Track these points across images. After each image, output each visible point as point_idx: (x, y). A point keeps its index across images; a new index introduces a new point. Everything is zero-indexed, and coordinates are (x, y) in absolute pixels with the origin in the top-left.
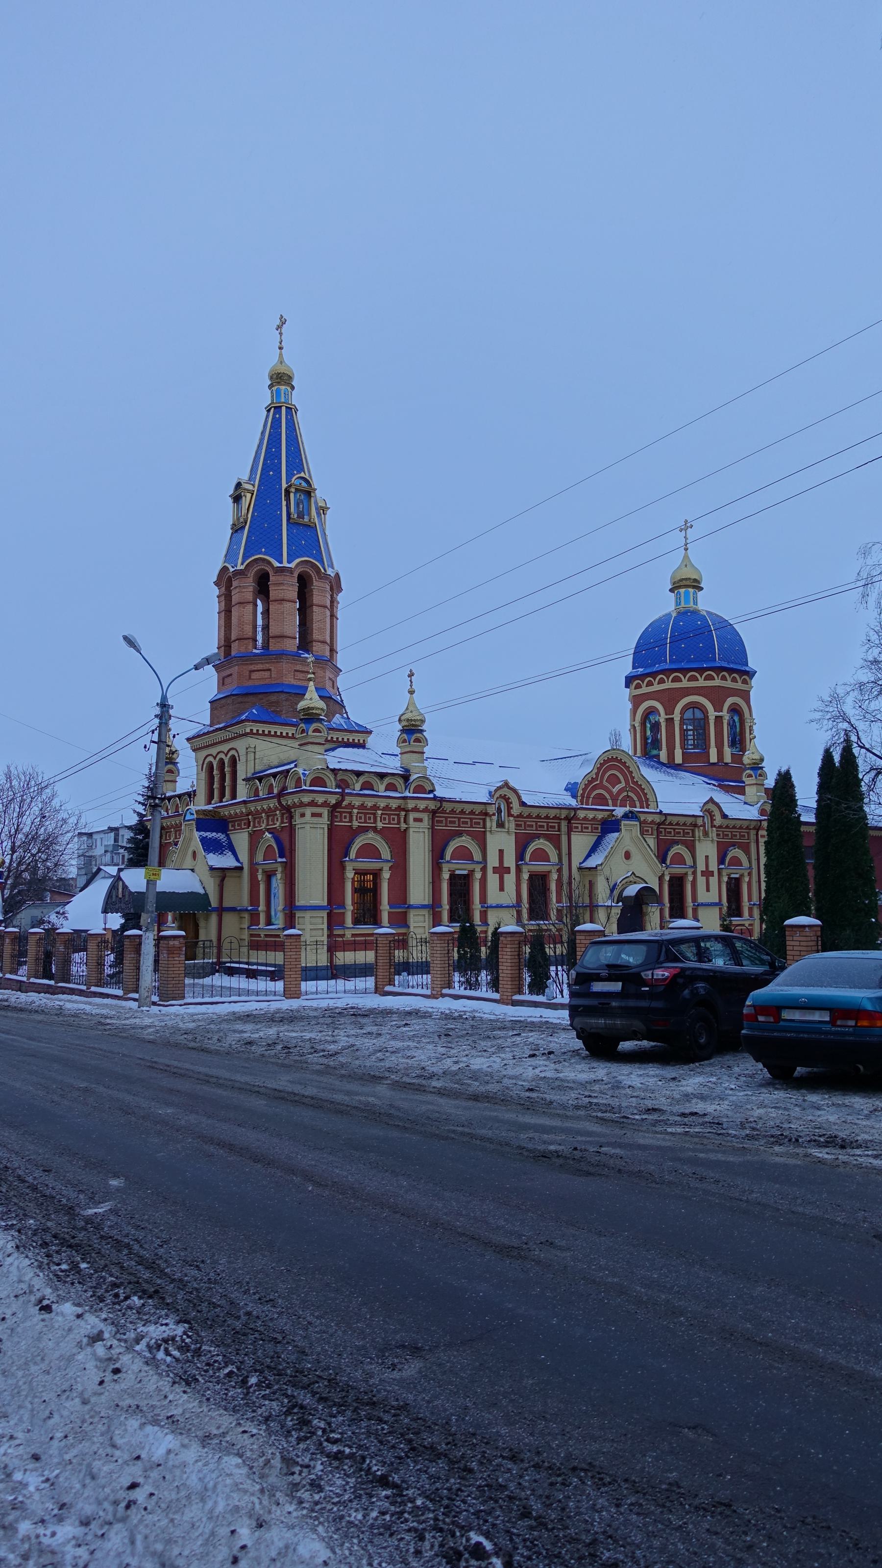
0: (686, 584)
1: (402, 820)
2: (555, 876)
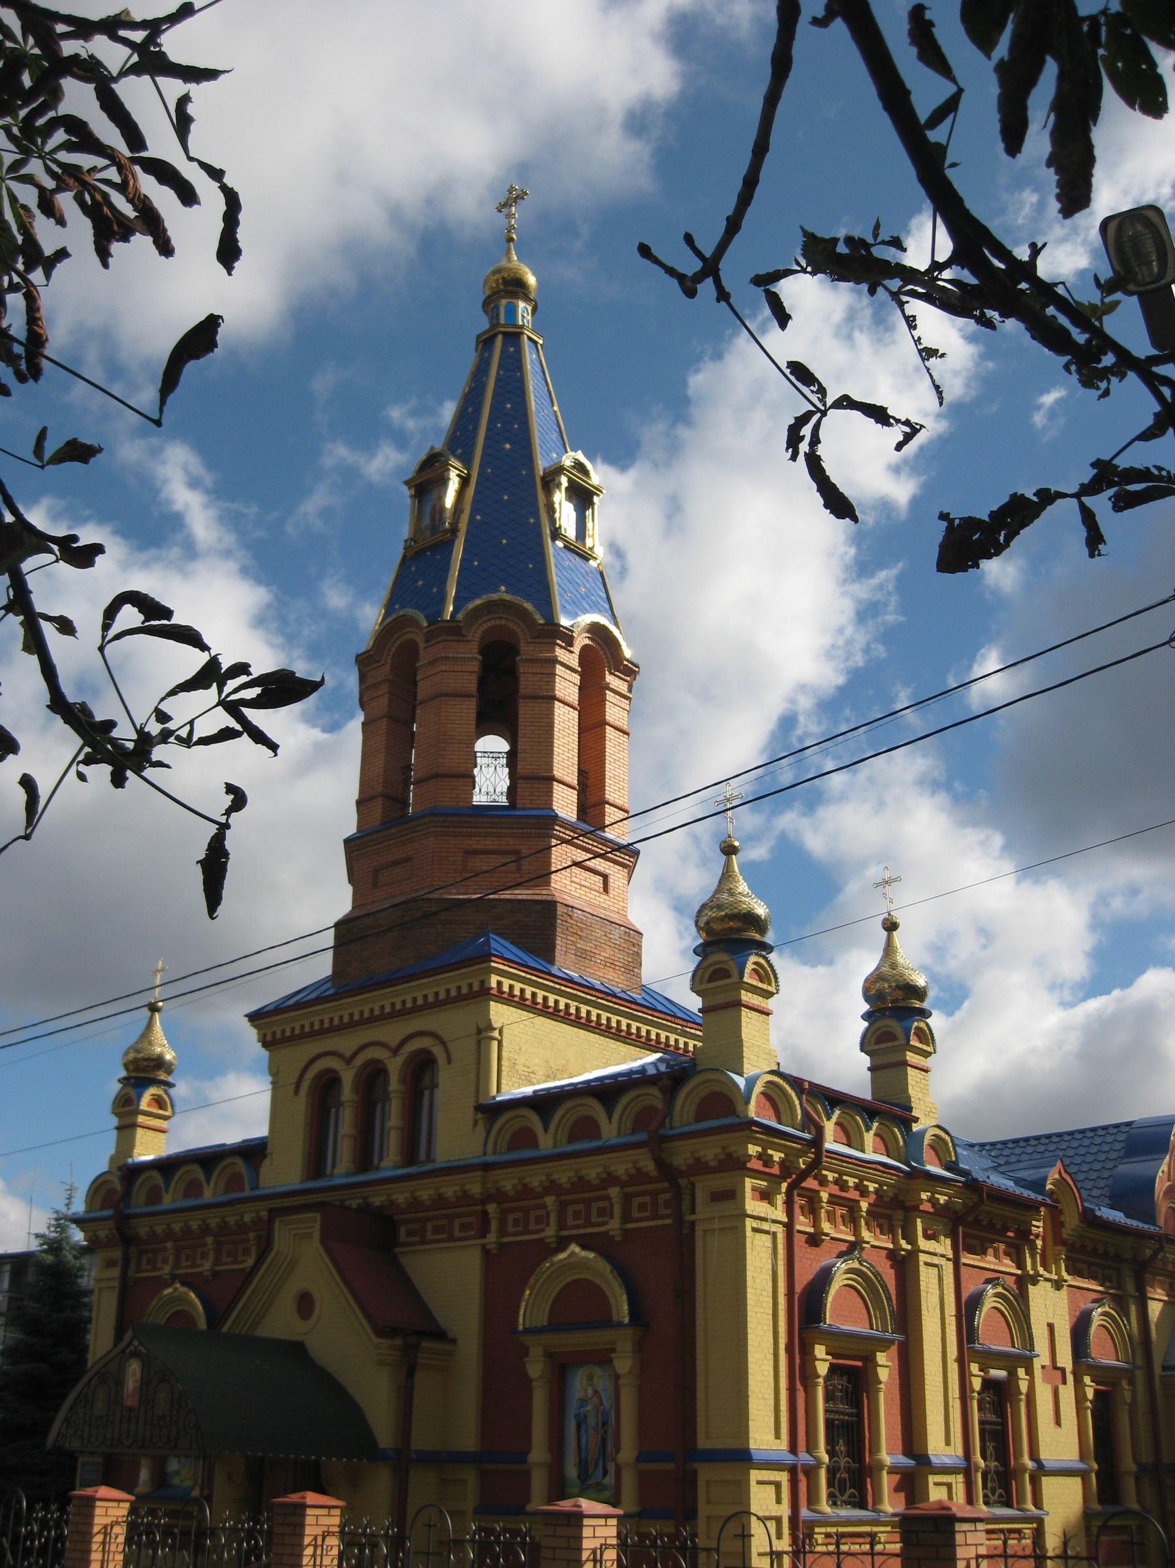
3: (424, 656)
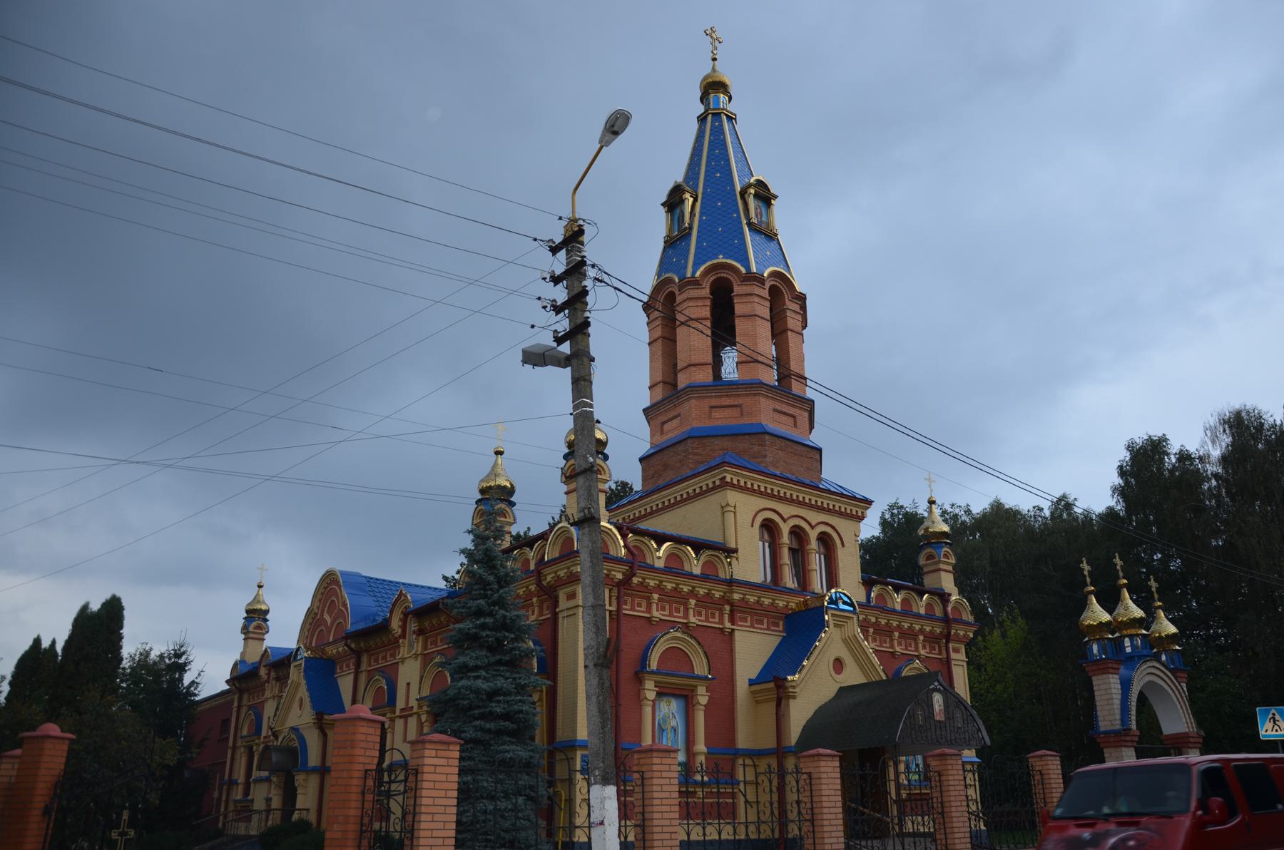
3: (679, 299)
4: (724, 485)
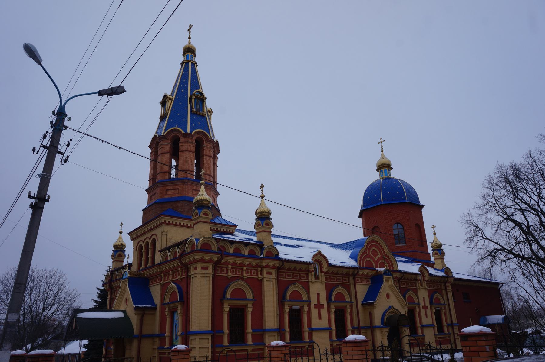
0: (384, 167)
1: (259, 273)
2: (349, 310)
4: (162, 224)
